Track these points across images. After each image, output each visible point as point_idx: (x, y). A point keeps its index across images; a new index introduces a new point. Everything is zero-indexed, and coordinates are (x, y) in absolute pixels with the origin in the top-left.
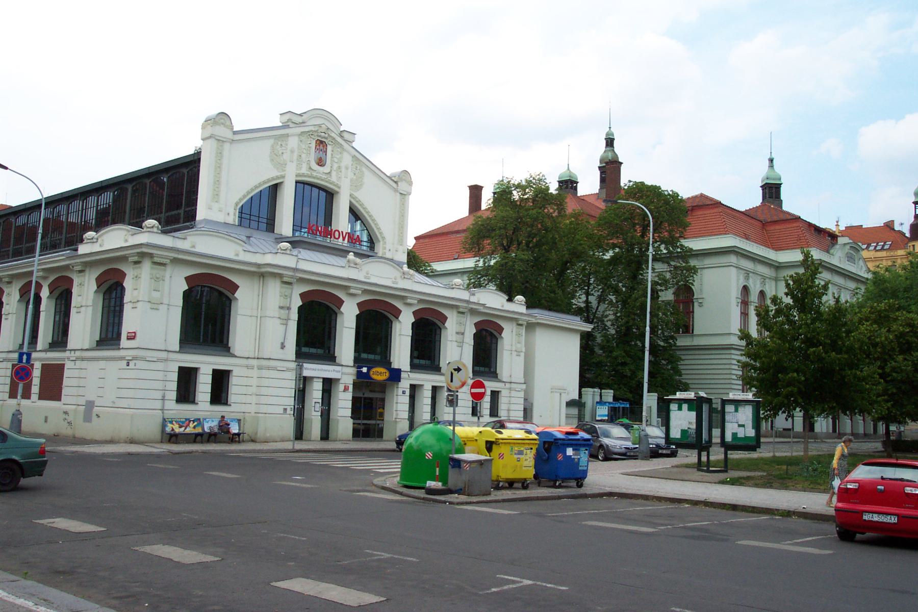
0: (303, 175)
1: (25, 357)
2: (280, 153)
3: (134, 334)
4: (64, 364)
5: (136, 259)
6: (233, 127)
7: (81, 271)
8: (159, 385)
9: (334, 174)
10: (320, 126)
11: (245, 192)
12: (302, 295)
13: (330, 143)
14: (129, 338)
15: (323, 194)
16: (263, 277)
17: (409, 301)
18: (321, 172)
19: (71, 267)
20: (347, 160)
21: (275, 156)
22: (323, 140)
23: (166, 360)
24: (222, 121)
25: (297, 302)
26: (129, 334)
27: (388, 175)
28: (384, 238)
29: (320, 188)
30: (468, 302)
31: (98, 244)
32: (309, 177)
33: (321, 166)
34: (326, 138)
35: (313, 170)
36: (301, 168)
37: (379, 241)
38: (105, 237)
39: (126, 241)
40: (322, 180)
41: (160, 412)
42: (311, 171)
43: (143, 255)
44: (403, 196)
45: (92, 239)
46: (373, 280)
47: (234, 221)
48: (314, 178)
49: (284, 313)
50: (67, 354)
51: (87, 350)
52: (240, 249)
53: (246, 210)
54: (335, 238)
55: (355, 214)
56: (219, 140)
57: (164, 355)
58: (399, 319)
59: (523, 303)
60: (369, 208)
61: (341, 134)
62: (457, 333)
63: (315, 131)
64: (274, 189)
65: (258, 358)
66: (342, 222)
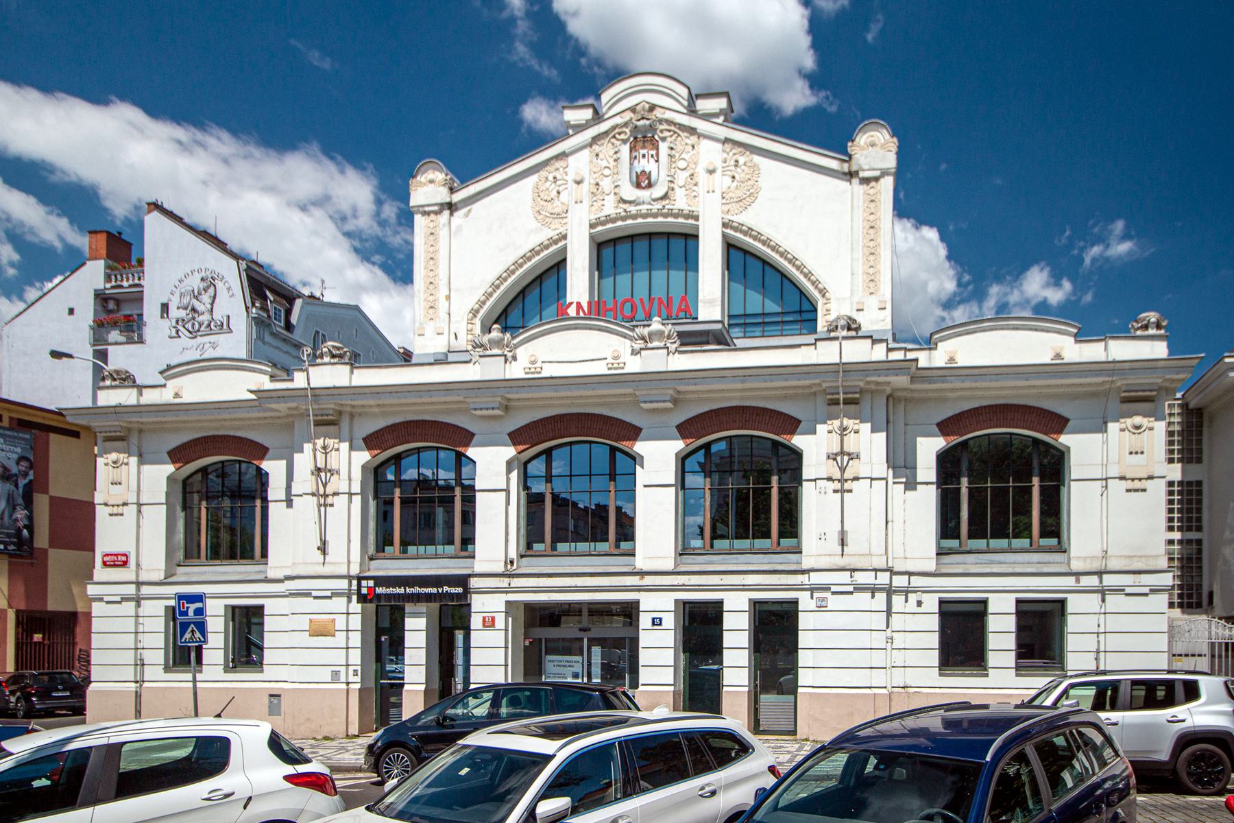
2: (554, 193)
10: (633, 109)
11: (486, 287)
13: (666, 134)
21: (545, 204)
32: (623, 219)
35: (625, 202)
40: (655, 216)
42: (625, 206)
44: (873, 184)
60: (777, 237)
63: (626, 125)
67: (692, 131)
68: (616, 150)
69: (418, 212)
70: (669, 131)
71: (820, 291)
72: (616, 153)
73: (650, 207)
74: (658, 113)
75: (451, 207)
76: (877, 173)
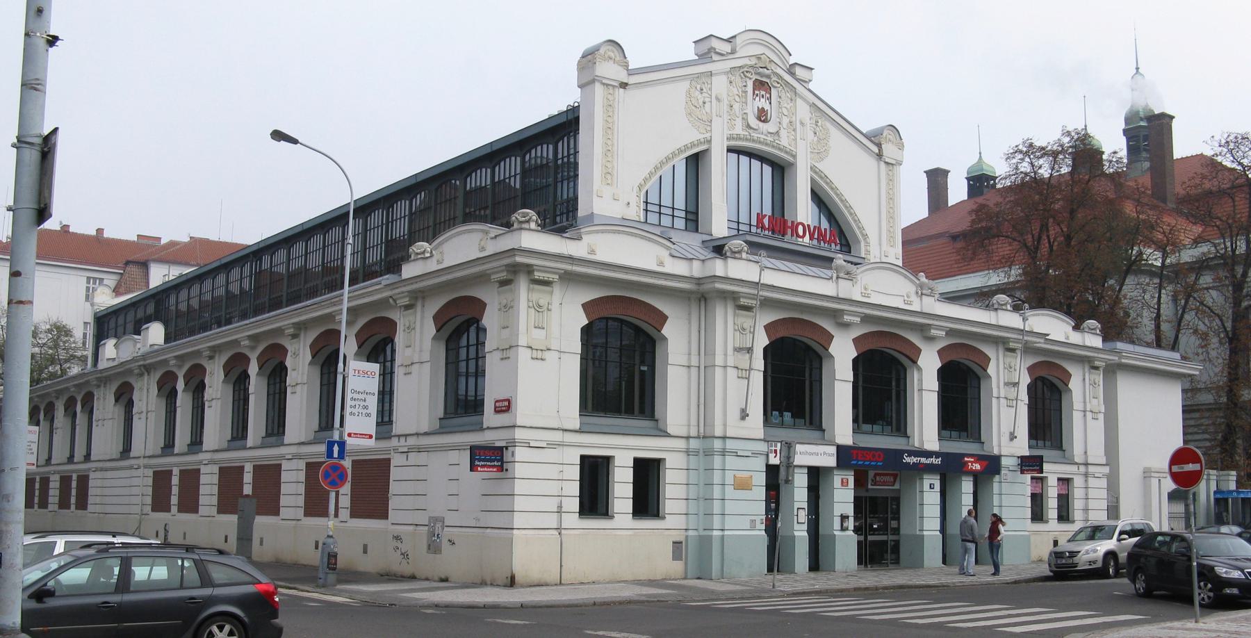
0: (739, 138)
1: (336, 448)
3: (507, 403)
4: (389, 460)
5: (503, 275)
6: (627, 63)
7: (408, 307)
8: (553, 488)
9: (783, 133)
12: (769, 328)
13: (776, 85)
14: (498, 411)
15: (768, 170)
16: (705, 300)
17: (934, 332)
18: (765, 132)
19: (391, 300)
20: (803, 111)
21: (693, 108)
22: (764, 79)
23: (561, 444)
24: (612, 55)
25: (762, 341)
26: (498, 404)
27: (865, 132)
28: (865, 236)
29: (763, 158)
30: (1021, 331)
31: (434, 259)
33: (764, 121)
34: (768, 77)
35: (751, 128)
36: (733, 127)
37: (859, 242)
38: (447, 247)
39: (483, 249)
40: (767, 145)
41: (555, 532)
42: (751, 131)
43: (515, 269)
45: (423, 253)
46: (875, 299)
47: (639, 216)
48: (754, 141)
49: (743, 360)
50: (394, 442)
51: (426, 434)
52: (664, 254)
53: (653, 198)
54: (798, 236)
55: (818, 198)
56: (607, 85)
57: (557, 437)
58: (919, 363)
59: (1098, 332)
61: (791, 70)
62: (1006, 384)
64: (696, 162)
65: (704, 437)
66: (804, 211)
67: (794, 89)
68: (745, 84)
69: (598, 81)
70: (778, 83)
71: (863, 235)
72: (745, 86)
73: (765, 137)
74: (773, 67)
75: (624, 85)
76: (894, 162)
